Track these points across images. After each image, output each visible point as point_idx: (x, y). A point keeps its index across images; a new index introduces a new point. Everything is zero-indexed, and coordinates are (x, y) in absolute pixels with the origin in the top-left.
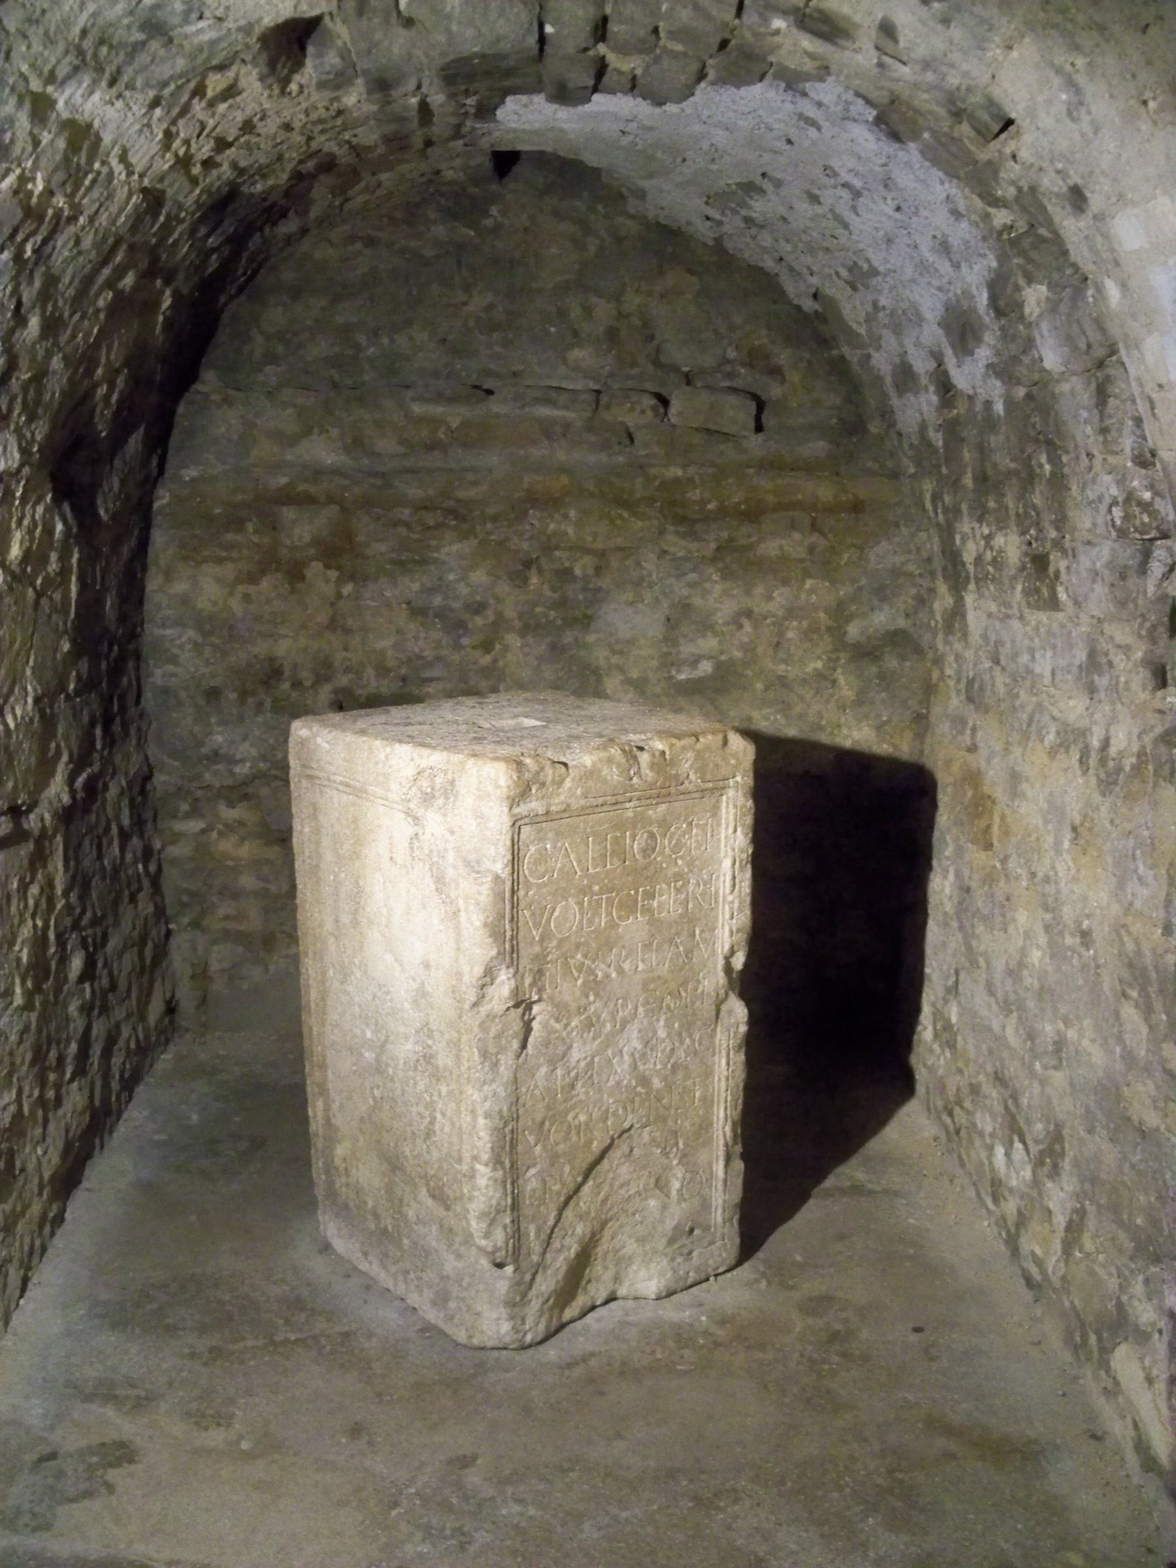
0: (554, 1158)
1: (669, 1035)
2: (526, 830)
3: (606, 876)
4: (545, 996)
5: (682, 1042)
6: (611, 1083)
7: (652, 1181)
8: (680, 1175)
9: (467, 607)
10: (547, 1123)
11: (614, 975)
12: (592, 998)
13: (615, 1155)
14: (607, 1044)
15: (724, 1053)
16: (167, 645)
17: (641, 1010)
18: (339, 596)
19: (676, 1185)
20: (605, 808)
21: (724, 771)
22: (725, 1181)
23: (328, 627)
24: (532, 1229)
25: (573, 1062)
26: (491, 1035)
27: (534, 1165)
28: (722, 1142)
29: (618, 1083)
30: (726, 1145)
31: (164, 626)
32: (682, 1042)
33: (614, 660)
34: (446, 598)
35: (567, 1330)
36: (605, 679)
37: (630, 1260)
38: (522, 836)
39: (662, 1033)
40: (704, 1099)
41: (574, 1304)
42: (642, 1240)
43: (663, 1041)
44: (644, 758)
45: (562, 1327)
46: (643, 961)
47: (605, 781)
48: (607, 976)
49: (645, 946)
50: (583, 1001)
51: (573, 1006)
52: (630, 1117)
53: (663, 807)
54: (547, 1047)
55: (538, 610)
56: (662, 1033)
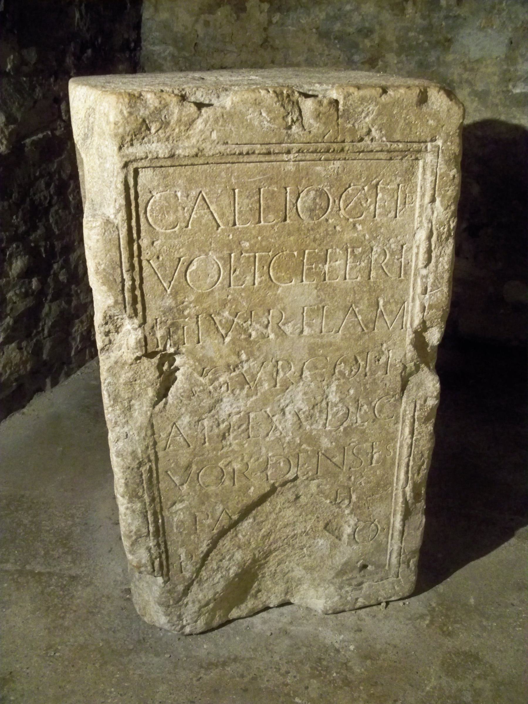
0: (204, 498)
1: (341, 400)
2: (145, 176)
3: (260, 233)
4: (183, 349)
5: (358, 408)
6: (271, 437)
7: (321, 524)
8: (352, 522)
9: (360, 31)
10: (194, 467)
11: (272, 336)
12: (244, 357)
13: (279, 500)
14: (265, 401)
15: (408, 422)
16: (155, 57)
17: (306, 373)
18: (270, 22)
19: (348, 530)
20: (253, 158)
21: (421, 132)
22: (402, 533)
23: (261, 46)
24: (182, 552)
25: (223, 415)
26: (121, 381)
27: (181, 501)
28: (401, 500)
29: (279, 439)
30: (406, 502)
31: (154, 44)
32: (358, 408)
33: (465, 76)
34: (344, 24)
35: (232, 625)
37: (300, 582)
38: (141, 180)
39: (333, 398)
40: (383, 461)
41: (243, 606)
42: (310, 569)
43: (336, 405)
44: (308, 105)
45: (229, 622)
46: (310, 325)
47: (250, 126)
48: (264, 337)
49: (313, 311)
50: (233, 359)
51: (221, 363)
52: (293, 470)
53: (338, 164)
54: (189, 398)
55: (411, 34)
56: (333, 398)
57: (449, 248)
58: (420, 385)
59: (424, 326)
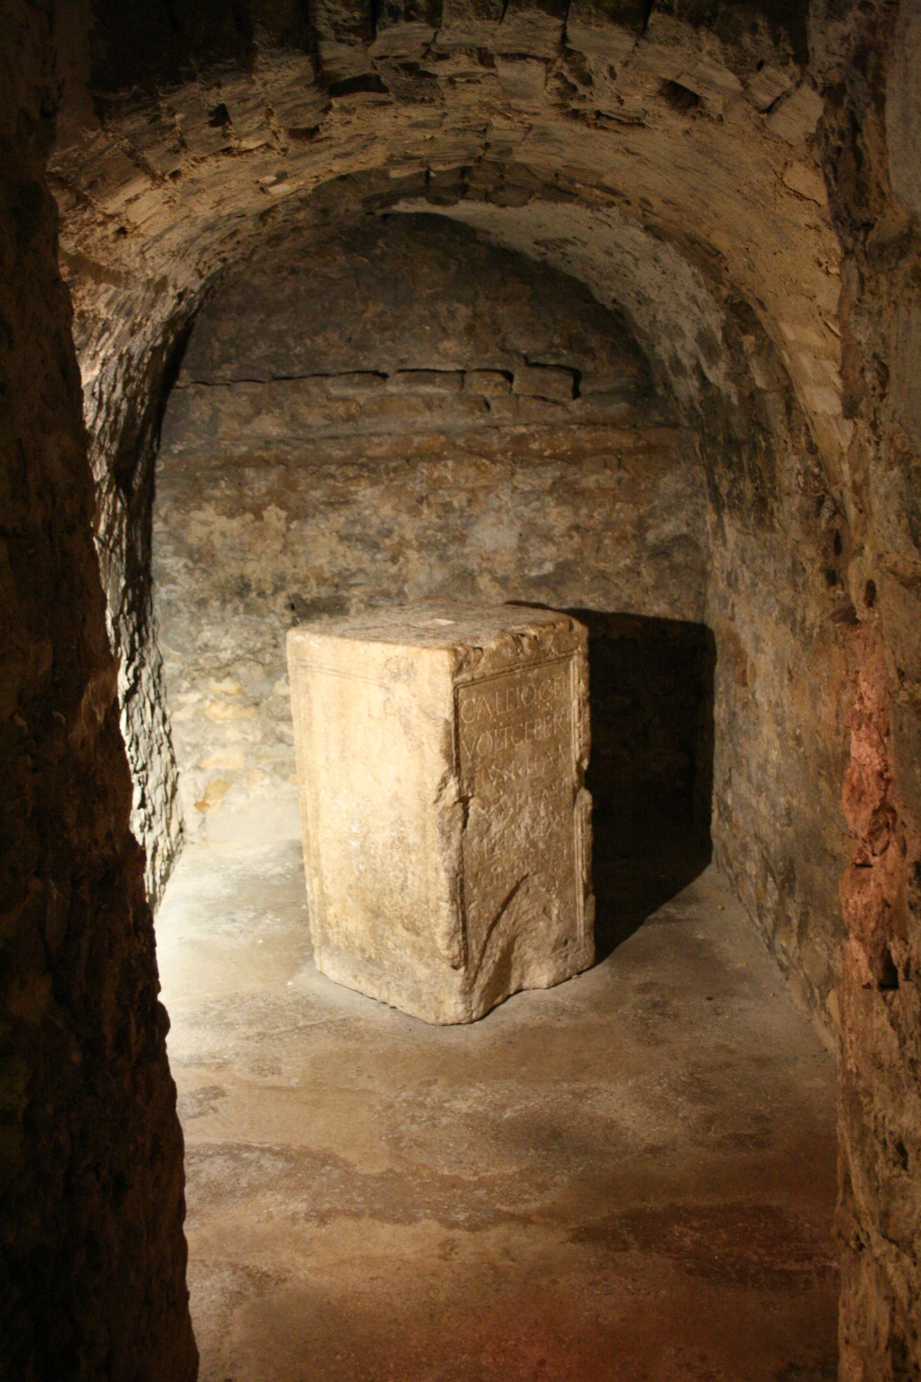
0: (484, 897)
6: (515, 847)
9: (379, 532)
11: (513, 777)
13: (519, 893)
18: (288, 529)
21: (571, 645)
23: (281, 552)
31: (165, 557)
33: (484, 565)
34: (364, 527)
36: (478, 579)
42: (537, 949)
44: (525, 641)
47: (504, 658)
50: (497, 795)
51: (491, 799)
55: (429, 532)
57: (588, 709)
58: (582, 798)
59: (581, 759)
